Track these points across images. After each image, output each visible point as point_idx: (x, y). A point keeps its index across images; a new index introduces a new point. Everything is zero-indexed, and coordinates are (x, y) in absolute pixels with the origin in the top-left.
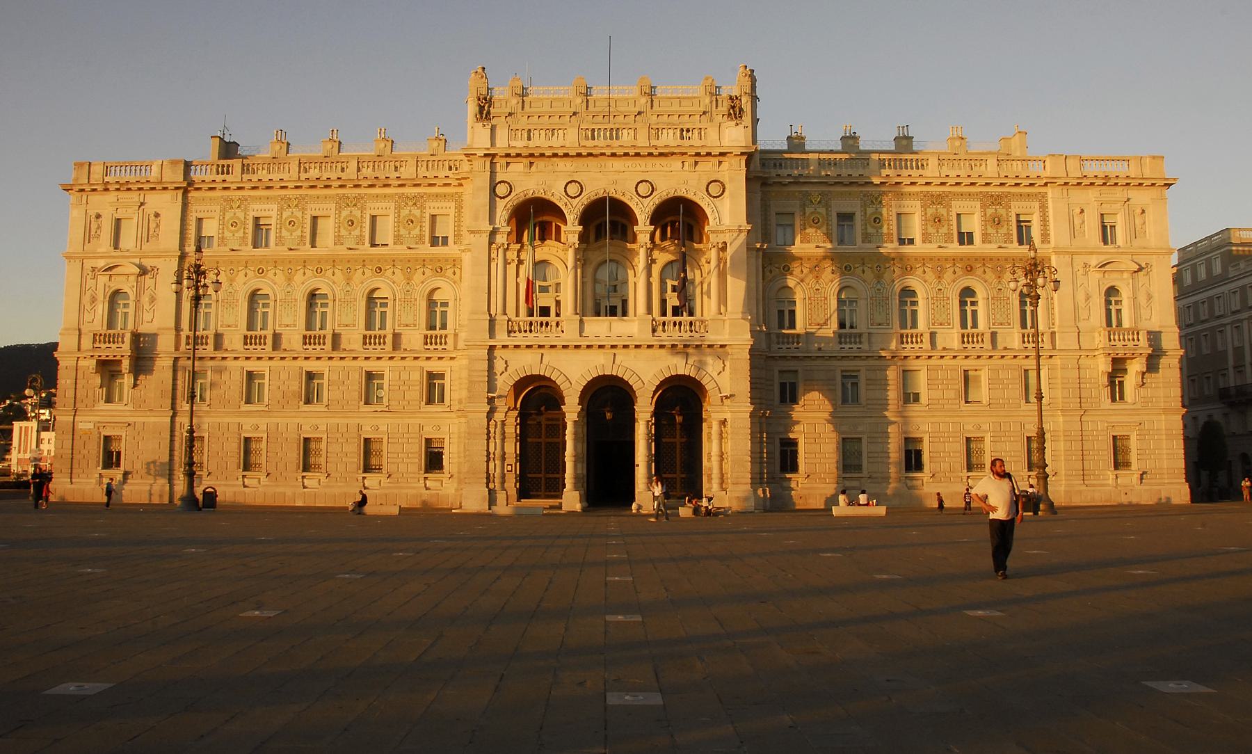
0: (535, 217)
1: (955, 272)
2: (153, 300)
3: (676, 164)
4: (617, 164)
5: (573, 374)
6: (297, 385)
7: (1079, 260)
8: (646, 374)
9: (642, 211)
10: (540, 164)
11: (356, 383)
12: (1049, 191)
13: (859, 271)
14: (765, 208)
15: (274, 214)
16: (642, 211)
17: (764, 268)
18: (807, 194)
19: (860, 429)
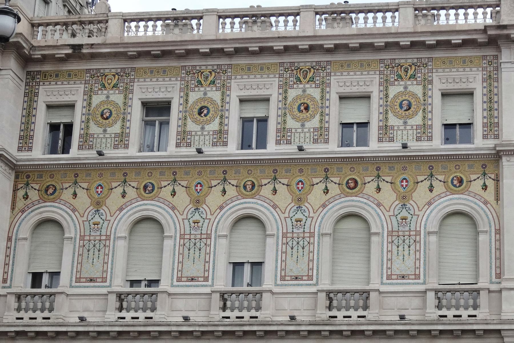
1: (326, 191)
14: (30, 97)
17: (15, 190)
18: (94, 74)
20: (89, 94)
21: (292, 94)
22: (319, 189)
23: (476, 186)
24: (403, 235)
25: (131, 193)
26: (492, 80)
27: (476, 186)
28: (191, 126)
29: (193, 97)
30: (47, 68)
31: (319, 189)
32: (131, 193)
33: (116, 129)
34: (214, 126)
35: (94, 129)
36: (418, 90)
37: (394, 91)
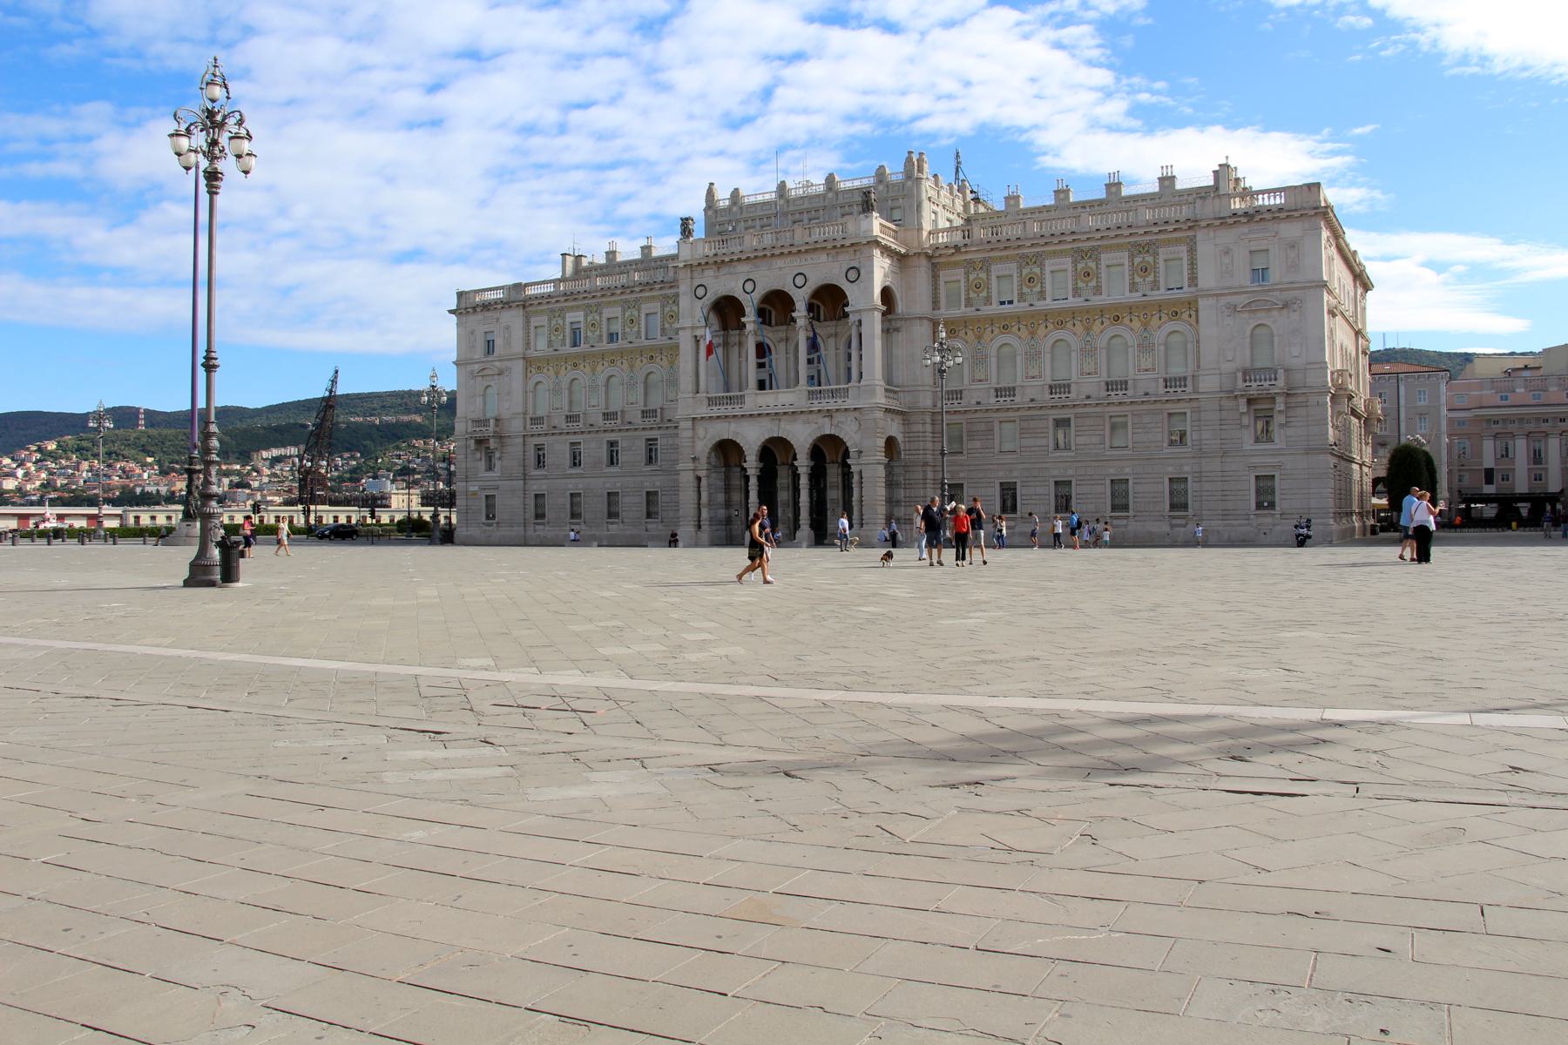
0: (727, 310)
2: (509, 393)
3: (823, 257)
4: (779, 263)
5: (751, 438)
6: (604, 453)
7: (1224, 301)
8: (801, 436)
9: (801, 298)
10: (724, 270)
11: (641, 446)
12: (1200, 235)
13: (1015, 329)
15: (582, 319)
16: (801, 298)
19: (1015, 474)
20: (967, 274)
21: (1080, 266)
22: (1098, 322)
23: (1185, 316)
24: (1146, 347)
25: (996, 331)
26: (1192, 251)
27: (1185, 316)
28: (1025, 290)
29: (1025, 271)
30: (942, 260)
31: (1098, 322)
32: (996, 331)
33: (984, 294)
34: (1038, 289)
35: (972, 295)
36: (1150, 259)
37: (1137, 260)
